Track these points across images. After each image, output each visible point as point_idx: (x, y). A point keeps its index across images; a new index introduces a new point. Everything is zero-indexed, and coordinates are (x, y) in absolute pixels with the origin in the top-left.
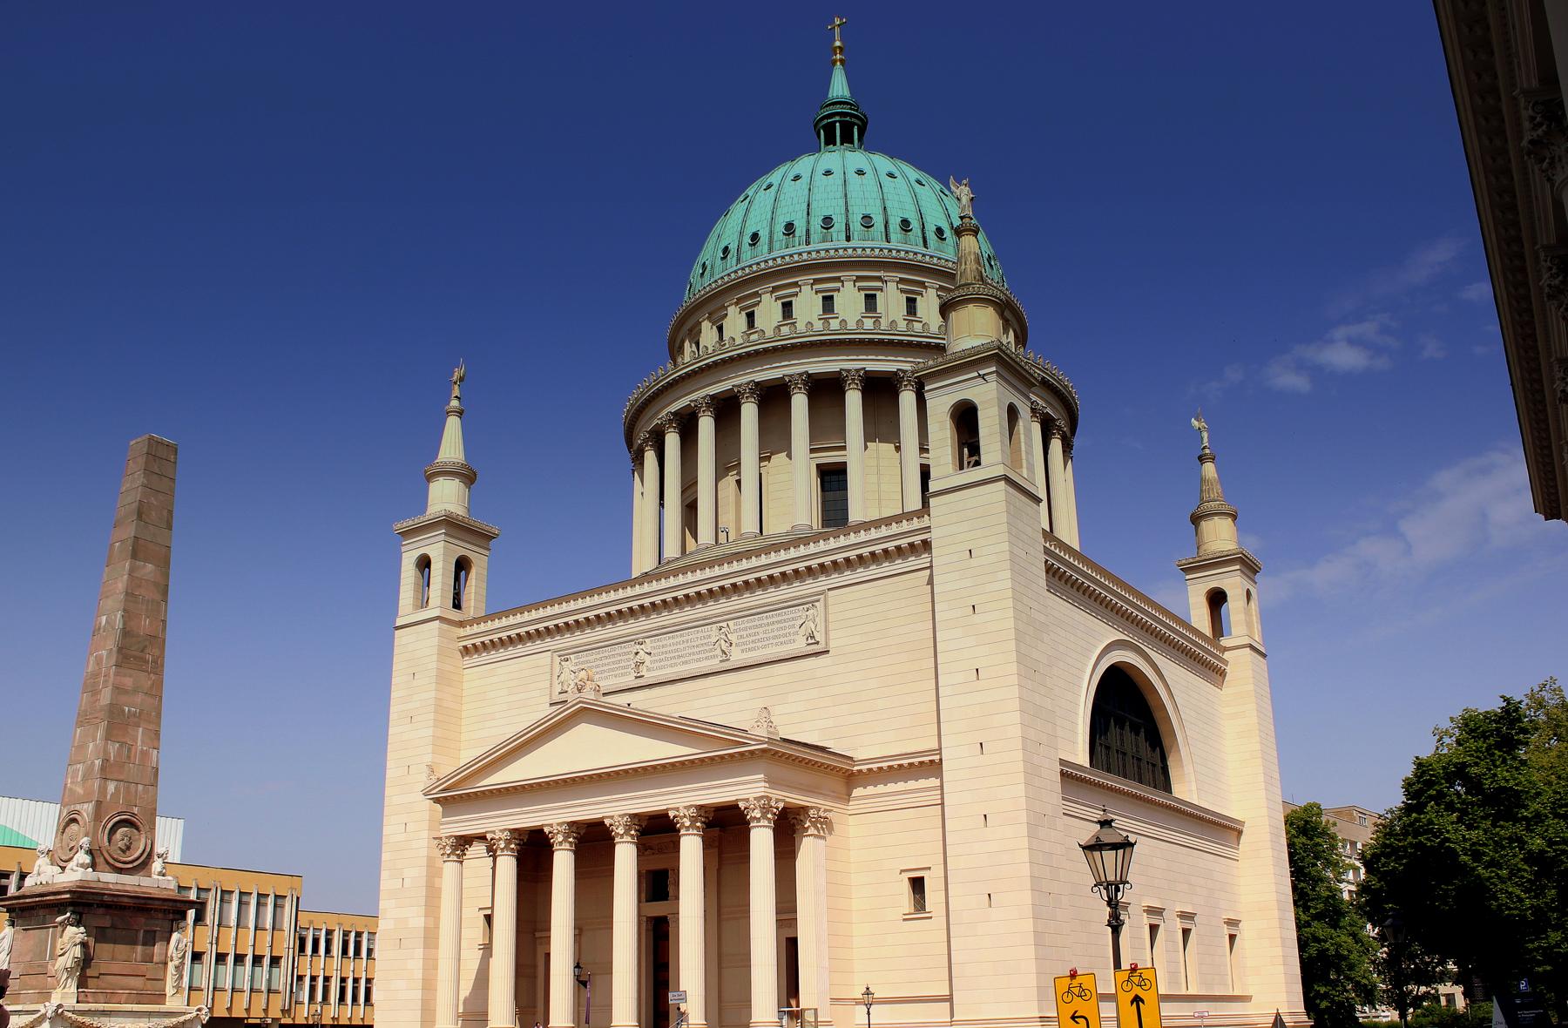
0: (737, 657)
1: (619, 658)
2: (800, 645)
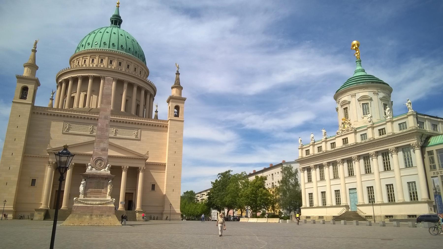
0: (118, 136)
1: (85, 128)
2: (134, 137)
